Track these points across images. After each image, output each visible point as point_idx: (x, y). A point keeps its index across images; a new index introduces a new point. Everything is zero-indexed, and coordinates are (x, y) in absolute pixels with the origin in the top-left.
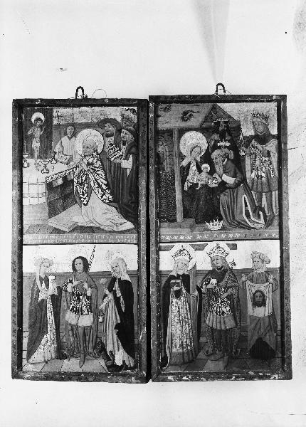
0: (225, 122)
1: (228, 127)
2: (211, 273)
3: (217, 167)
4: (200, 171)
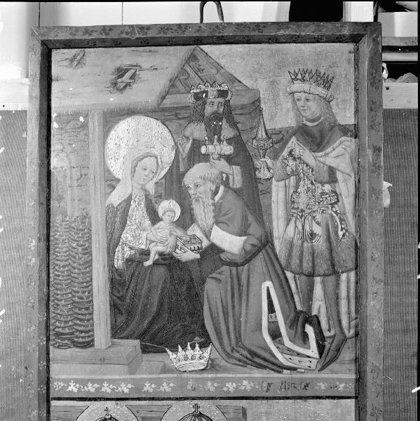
0: (223, 94)
1: (227, 103)
3: (198, 210)
4: (155, 218)
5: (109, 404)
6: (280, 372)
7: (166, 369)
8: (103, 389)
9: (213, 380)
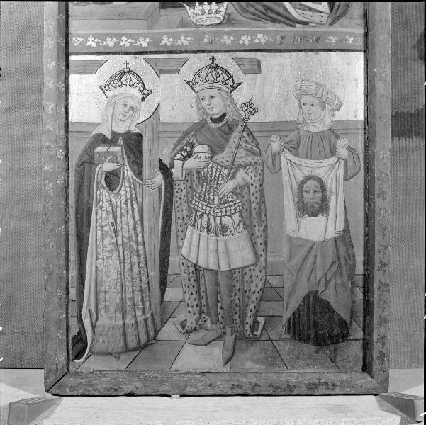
2: (199, 127)
5: (127, 57)
6: (293, 26)
7: (184, 24)
8: (122, 44)
9: (229, 34)
